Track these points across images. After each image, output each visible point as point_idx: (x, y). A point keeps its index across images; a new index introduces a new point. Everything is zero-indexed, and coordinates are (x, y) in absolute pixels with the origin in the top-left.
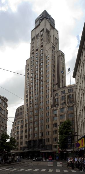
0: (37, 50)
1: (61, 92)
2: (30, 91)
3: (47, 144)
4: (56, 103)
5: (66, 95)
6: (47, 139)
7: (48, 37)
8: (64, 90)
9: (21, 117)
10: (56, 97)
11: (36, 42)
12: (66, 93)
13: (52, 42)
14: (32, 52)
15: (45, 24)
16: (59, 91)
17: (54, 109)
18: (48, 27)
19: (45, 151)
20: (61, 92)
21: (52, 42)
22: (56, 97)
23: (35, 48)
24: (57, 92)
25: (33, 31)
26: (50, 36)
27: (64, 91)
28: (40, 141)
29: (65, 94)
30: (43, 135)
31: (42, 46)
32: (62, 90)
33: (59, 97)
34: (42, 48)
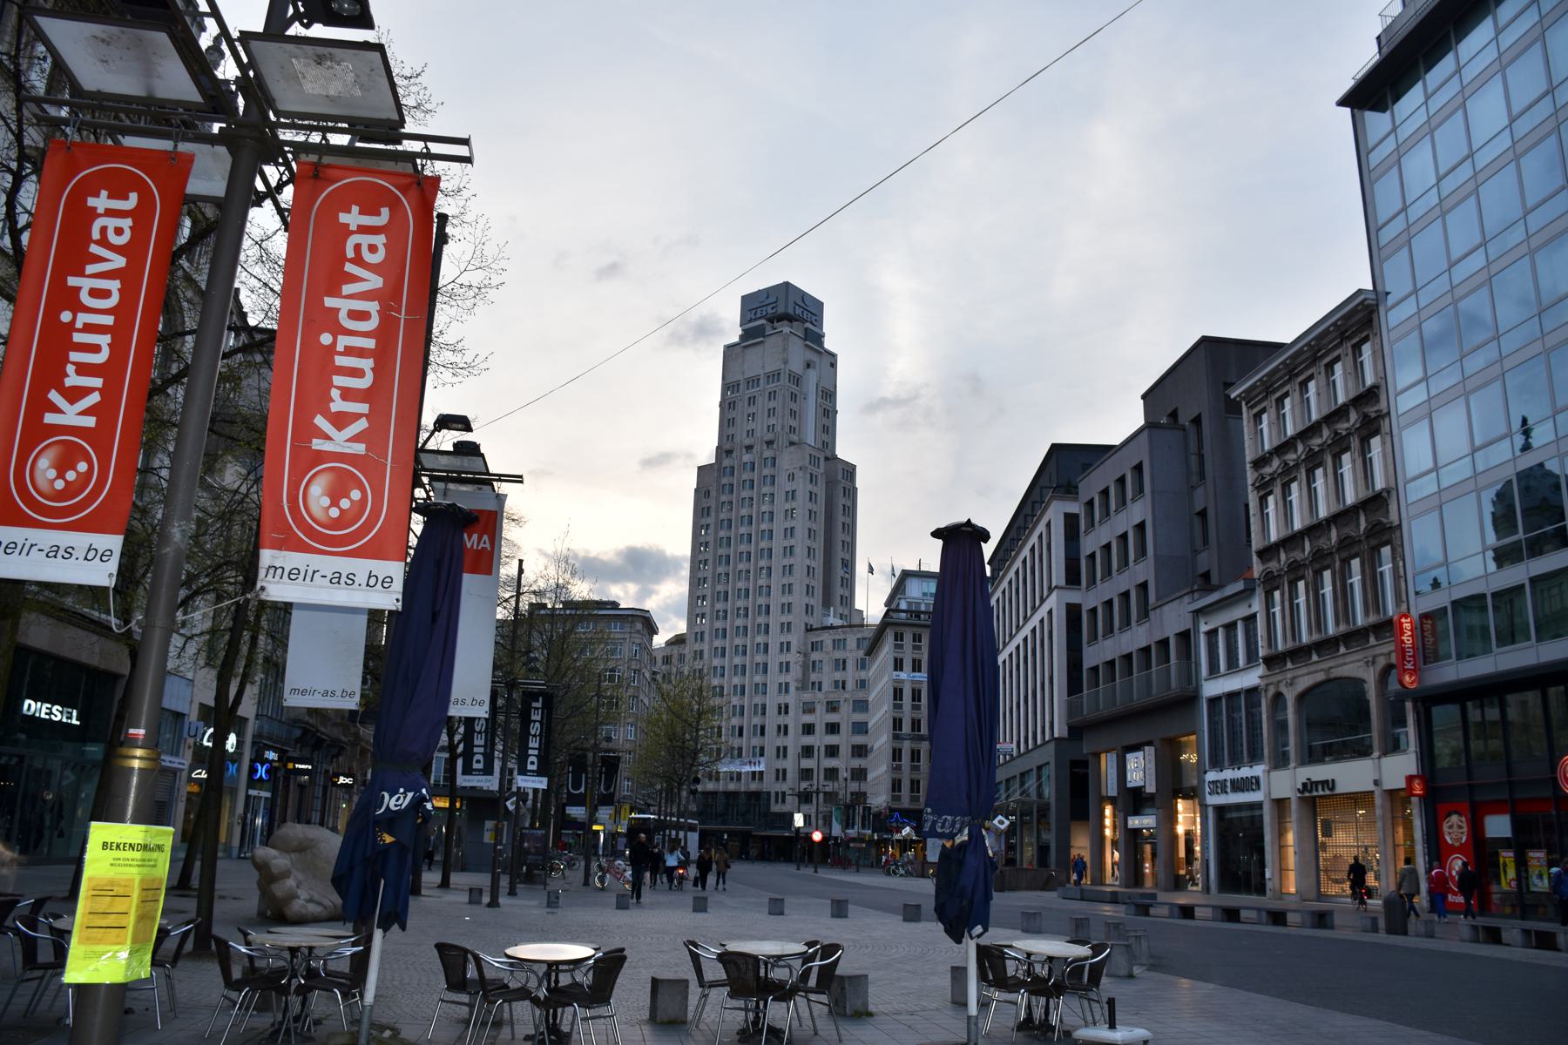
0: (749, 448)
1: (834, 640)
3: (776, 808)
6: (777, 793)
8: (842, 637)
11: (743, 408)
12: (848, 648)
13: (810, 440)
14: (727, 447)
15: (783, 351)
18: (798, 354)
19: (769, 833)
20: (834, 640)
21: (810, 440)
22: (815, 656)
23: (741, 438)
24: (819, 639)
26: (803, 396)
27: (845, 640)
28: (756, 795)
31: (769, 443)
32: (837, 637)
34: (768, 453)
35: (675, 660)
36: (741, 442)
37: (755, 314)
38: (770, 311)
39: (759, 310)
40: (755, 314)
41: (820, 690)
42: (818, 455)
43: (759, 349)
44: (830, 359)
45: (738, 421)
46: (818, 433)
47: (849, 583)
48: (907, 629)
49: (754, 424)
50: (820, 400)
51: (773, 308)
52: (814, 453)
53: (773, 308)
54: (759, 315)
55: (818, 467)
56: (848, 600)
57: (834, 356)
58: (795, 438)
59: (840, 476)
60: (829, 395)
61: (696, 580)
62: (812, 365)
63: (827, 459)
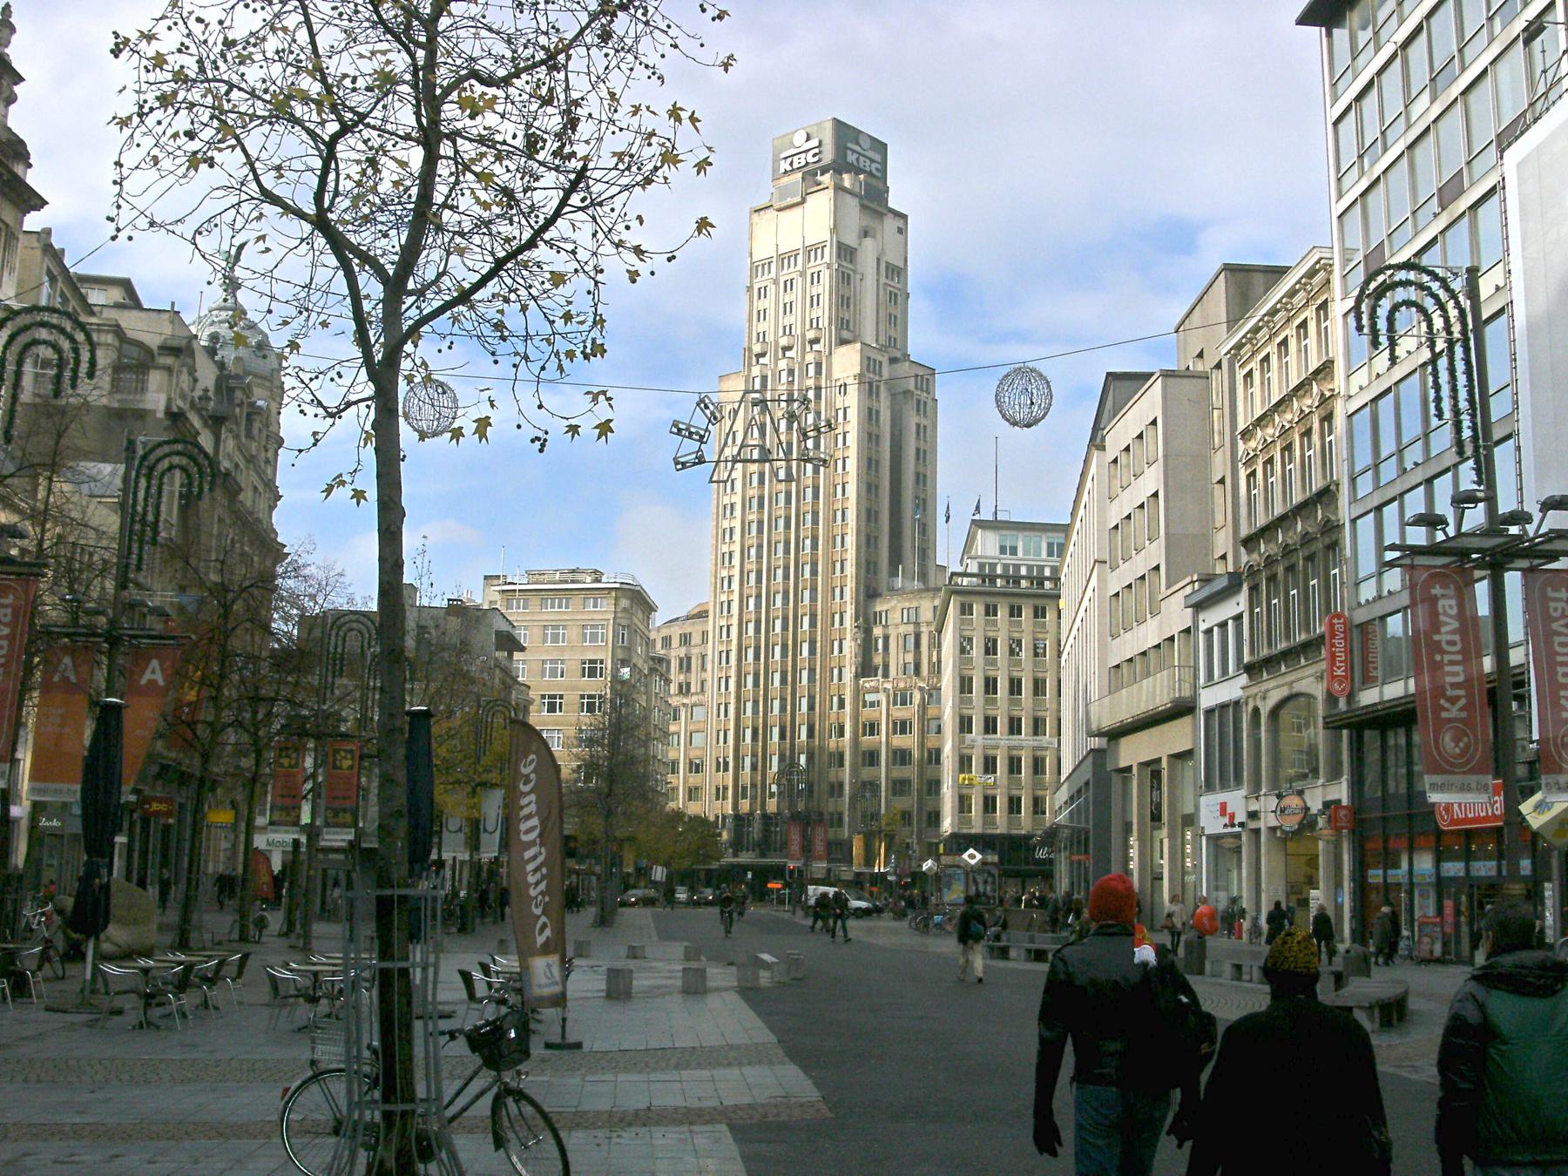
2: (747, 567)
4: (878, 660)
5: (924, 629)
7: (849, 284)
8: (915, 604)
9: (688, 685)
10: (878, 631)
14: (757, 349)
16: (893, 603)
17: (867, 685)
24: (885, 607)
25: (762, 213)
26: (858, 277)
29: (917, 624)
30: (815, 793)
32: (907, 605)
33: (892, 632)
35: (696, 639)
36: (776, 342)
37: (791, 164)
38: (811, 159)
39: (796, 158)
40: (791, 164)
41: (886, 675)
42: (879, 358)
43: (797, 211)
44: (900, 223)
45: (771, 314)
46: (882, 327)
47: (926, 530)
48: (977, 598)
49: (793, 317)
50: (883, 280)
51: (814, 156)
52: (873, 356)
53: (814, 156)
54: (796, 165)
55: (881, 376)
56: (926, 552)
57: (904, 217)
58: (845, 334)
59: (912, 387)
60: (896, 272)
61: (720, 531)
62: (871, 232)
63: (893, 360)
